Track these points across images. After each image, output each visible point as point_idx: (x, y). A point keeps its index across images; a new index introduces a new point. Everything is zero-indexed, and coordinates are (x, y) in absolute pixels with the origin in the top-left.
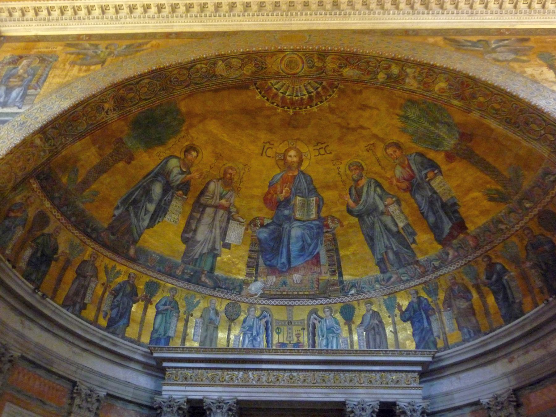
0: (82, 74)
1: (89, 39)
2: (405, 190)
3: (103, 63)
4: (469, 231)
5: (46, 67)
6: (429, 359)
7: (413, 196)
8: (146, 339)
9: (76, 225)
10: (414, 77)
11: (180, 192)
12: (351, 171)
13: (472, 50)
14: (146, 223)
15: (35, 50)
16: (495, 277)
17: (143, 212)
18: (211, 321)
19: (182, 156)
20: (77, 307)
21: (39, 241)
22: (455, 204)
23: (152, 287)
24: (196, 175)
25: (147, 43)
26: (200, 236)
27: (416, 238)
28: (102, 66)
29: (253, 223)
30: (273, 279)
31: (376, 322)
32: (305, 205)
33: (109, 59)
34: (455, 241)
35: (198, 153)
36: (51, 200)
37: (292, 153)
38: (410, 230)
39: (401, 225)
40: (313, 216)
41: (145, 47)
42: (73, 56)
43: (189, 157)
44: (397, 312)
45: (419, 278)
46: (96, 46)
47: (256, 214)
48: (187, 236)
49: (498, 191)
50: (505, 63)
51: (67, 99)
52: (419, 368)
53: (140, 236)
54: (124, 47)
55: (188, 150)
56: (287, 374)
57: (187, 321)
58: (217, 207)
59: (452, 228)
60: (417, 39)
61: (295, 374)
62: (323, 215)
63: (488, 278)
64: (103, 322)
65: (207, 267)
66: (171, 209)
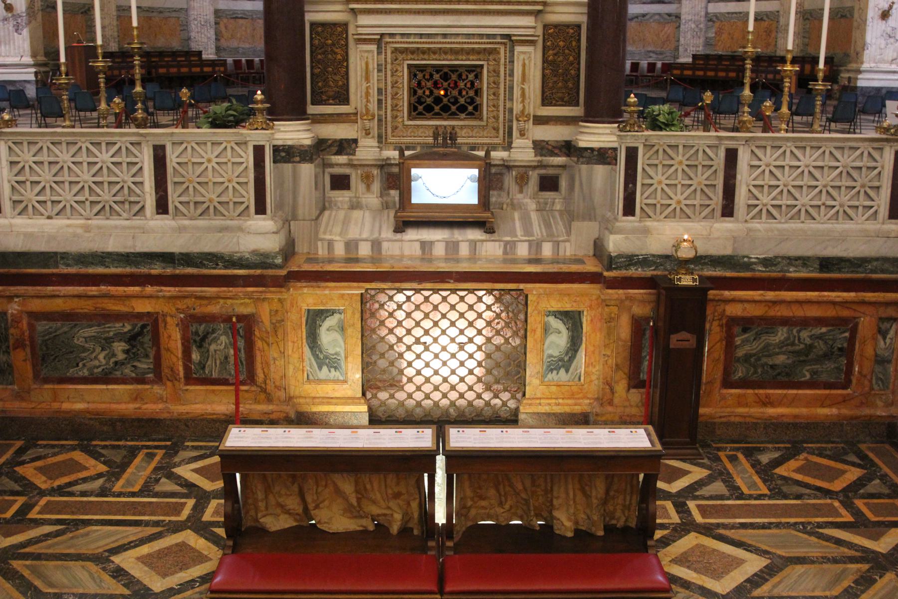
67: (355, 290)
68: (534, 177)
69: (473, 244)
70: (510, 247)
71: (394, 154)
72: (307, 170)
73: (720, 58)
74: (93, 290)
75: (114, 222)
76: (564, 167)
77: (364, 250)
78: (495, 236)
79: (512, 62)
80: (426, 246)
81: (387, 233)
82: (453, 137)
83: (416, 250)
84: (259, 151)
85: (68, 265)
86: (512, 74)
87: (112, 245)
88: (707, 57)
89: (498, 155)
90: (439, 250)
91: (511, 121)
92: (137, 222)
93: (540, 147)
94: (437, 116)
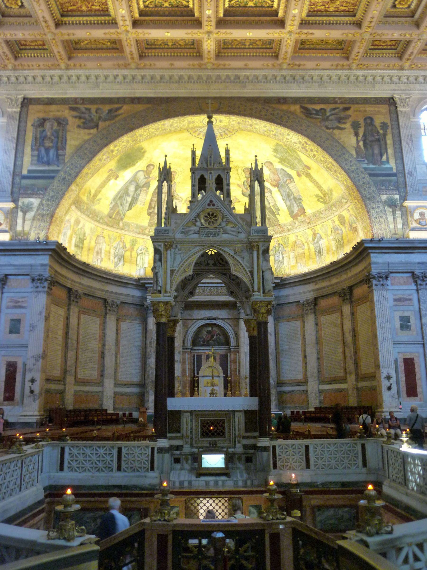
0: (87, 138)
1: (83, 103)
2: (275, 186)
3: (97, 126)
4: (306, 214)
5: (63, 130)
6: (279, 281)
7: (279, 191)
9: (92, 218)
10: (280, 134)
11: (145, 188)
12: (245, 172)
13: (315, 118)
14: (127, 208)
15: (52, 113)
16: (316, 240)
17: (125, 202)
19: (145, 169)
20: (99, 261)
21: (77, 233)
22: (300, 199)
23: (133, 243)
25: (120, 108)
27: (279, 212)
28: (98, 129)
33: (100, 123)
34: (299, 218)
35: (154, 166)
36: (80, 211)
38: (276, 208)
39: (272, 204)
41: (120, 112)
42: (77, 120)
43: (149, 169)
45: (280, 233)
46: (89, 110)
48: (150, 211)
49: (322, 198)
50: (331, 130)
51: (83, 159)
52: (274, 285)
53: (124, 216)
54: (107, 112)
56: (209, 288)
59: (298, 210)
60: (284, 107)
61: (212, 288)
63: (313, 240)
66: (140, 198)
67: (183, 498)
68: (243, 457)
69: (223, 481)
70: (236, 483)
71: (196, 450)
72: (167, 456)
73: (326, 408)
74: (93, 499)
75: (102, 474)
76: (253, 453)
77: (186, 484)
78: (230, 479)
79: (235, 418)
80: (207, 483)
81: (193, 478)
82: (216, 444)
83: (204, 483)
84: (153, 449)
85: (85, 490)
86: (235, 422)
87: (101, 482)
88: (321, 408)
89: (231, 450)
90: (212, 484)
91: (235, 438)
92: (111, 474)
93: (245, 447)
94: (210, 437)
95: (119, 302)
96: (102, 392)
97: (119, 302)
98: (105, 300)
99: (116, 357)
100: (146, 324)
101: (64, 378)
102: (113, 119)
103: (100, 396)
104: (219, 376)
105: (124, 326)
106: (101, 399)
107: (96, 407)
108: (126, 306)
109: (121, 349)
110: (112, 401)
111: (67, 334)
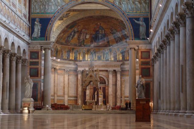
0: (60, 23)
3: (63, 19)
8: (73, 59)
14: (71, 39)
18: (84, 53)
24: (80, 29)
25: (69, 13)
26: (81, 38)
29: (91, 34)
30: (96, 44)
31: (115, 52)
32: (102, 31)
37: (99, 23)
40: (103, 33)
41: (70, 14)
44: (119, 51)
47: (92, 33)
55: (78, 27)
57: (80, 54)
58: (84, 33)
62: (106, 32)
64: (66, 58)
65: (83, 43)
95: (69, 70)
96: (64, 99)
97: (69, 70)
98: (64, 70)
99: (68, 88)
100: (78, 77)
101: (54, 95)
102: (67, 17)
103: (64, 100)
104: (102, 94)
105: (70, 77)
106: (64, 101)
107: (63, 103)
108: (71, 71)
109: (70, 85)
110: (67, 102)
111: (55, 82)
